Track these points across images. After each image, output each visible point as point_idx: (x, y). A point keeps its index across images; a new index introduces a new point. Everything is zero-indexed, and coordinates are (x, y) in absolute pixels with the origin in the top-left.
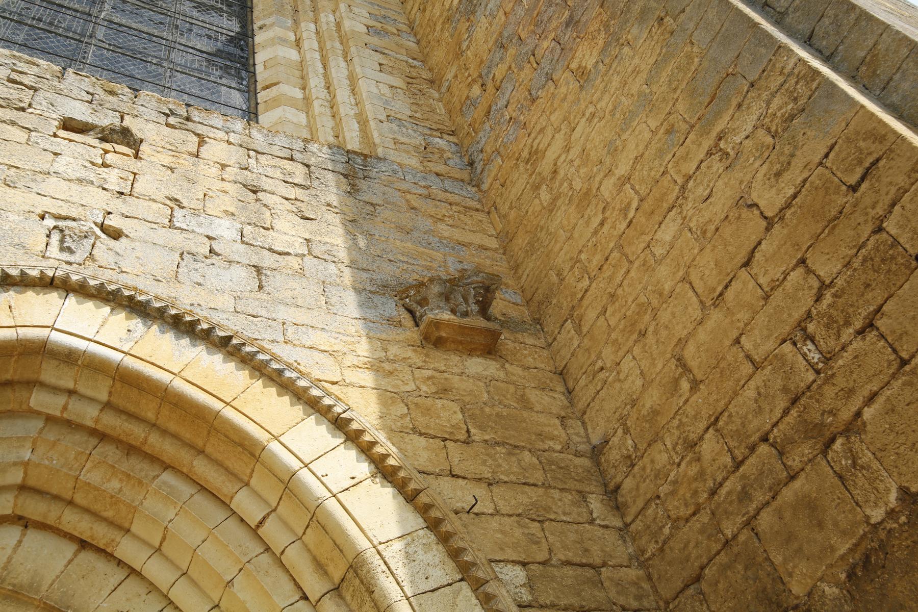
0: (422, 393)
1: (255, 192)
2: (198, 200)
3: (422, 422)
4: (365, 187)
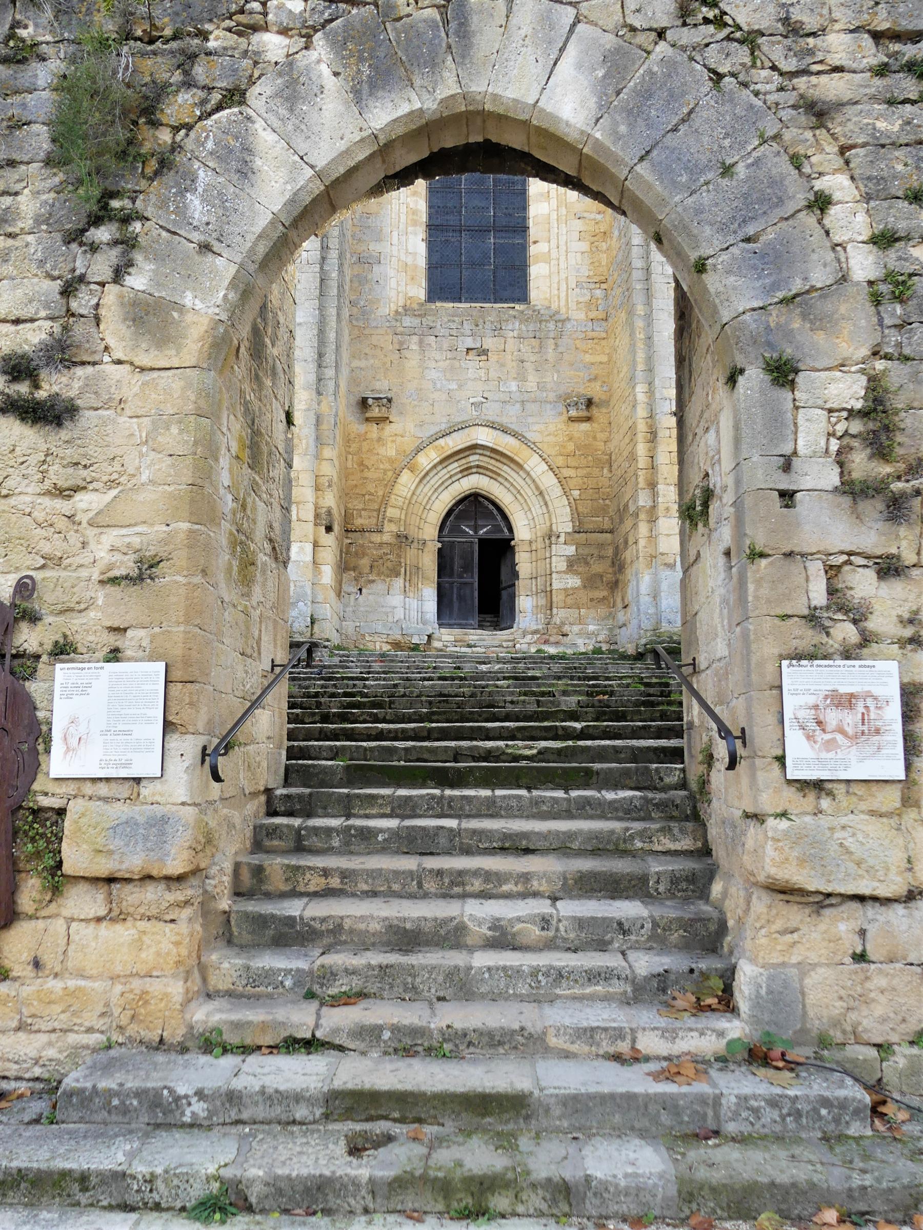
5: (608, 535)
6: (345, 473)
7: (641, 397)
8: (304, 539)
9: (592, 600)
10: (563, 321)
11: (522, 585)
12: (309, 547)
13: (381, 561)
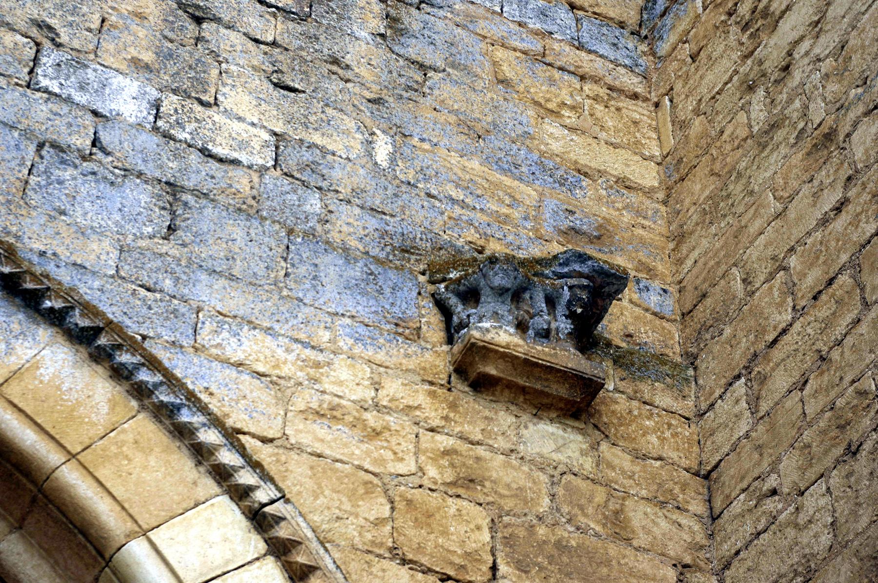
0: (426, 482)
1: (198, 21)
2: (90, 30)
3: (412, 536)
4: (416, 27)
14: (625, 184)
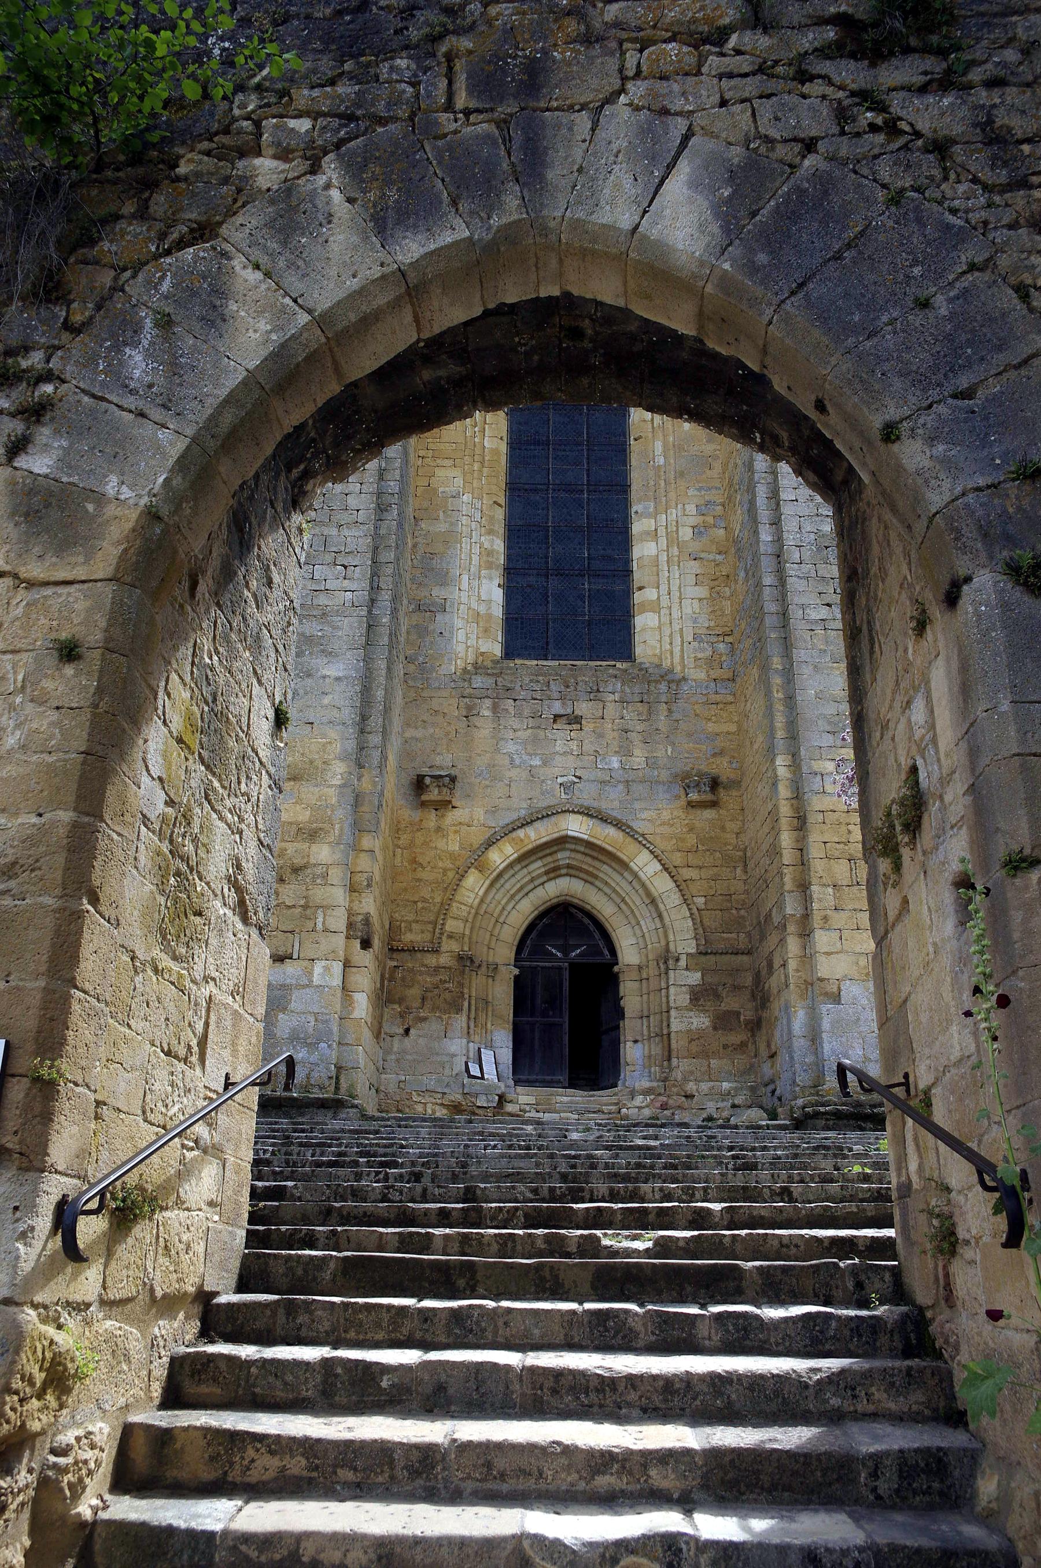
5: (745, 958)
6: (392, 874)
7: (782, 772)
8: (331, 957)
9: (725, 1047)
10: (680, 681)
11: (630, 1027)
12: (337, 967)
13: (436, 991)
14: (728, 733)
